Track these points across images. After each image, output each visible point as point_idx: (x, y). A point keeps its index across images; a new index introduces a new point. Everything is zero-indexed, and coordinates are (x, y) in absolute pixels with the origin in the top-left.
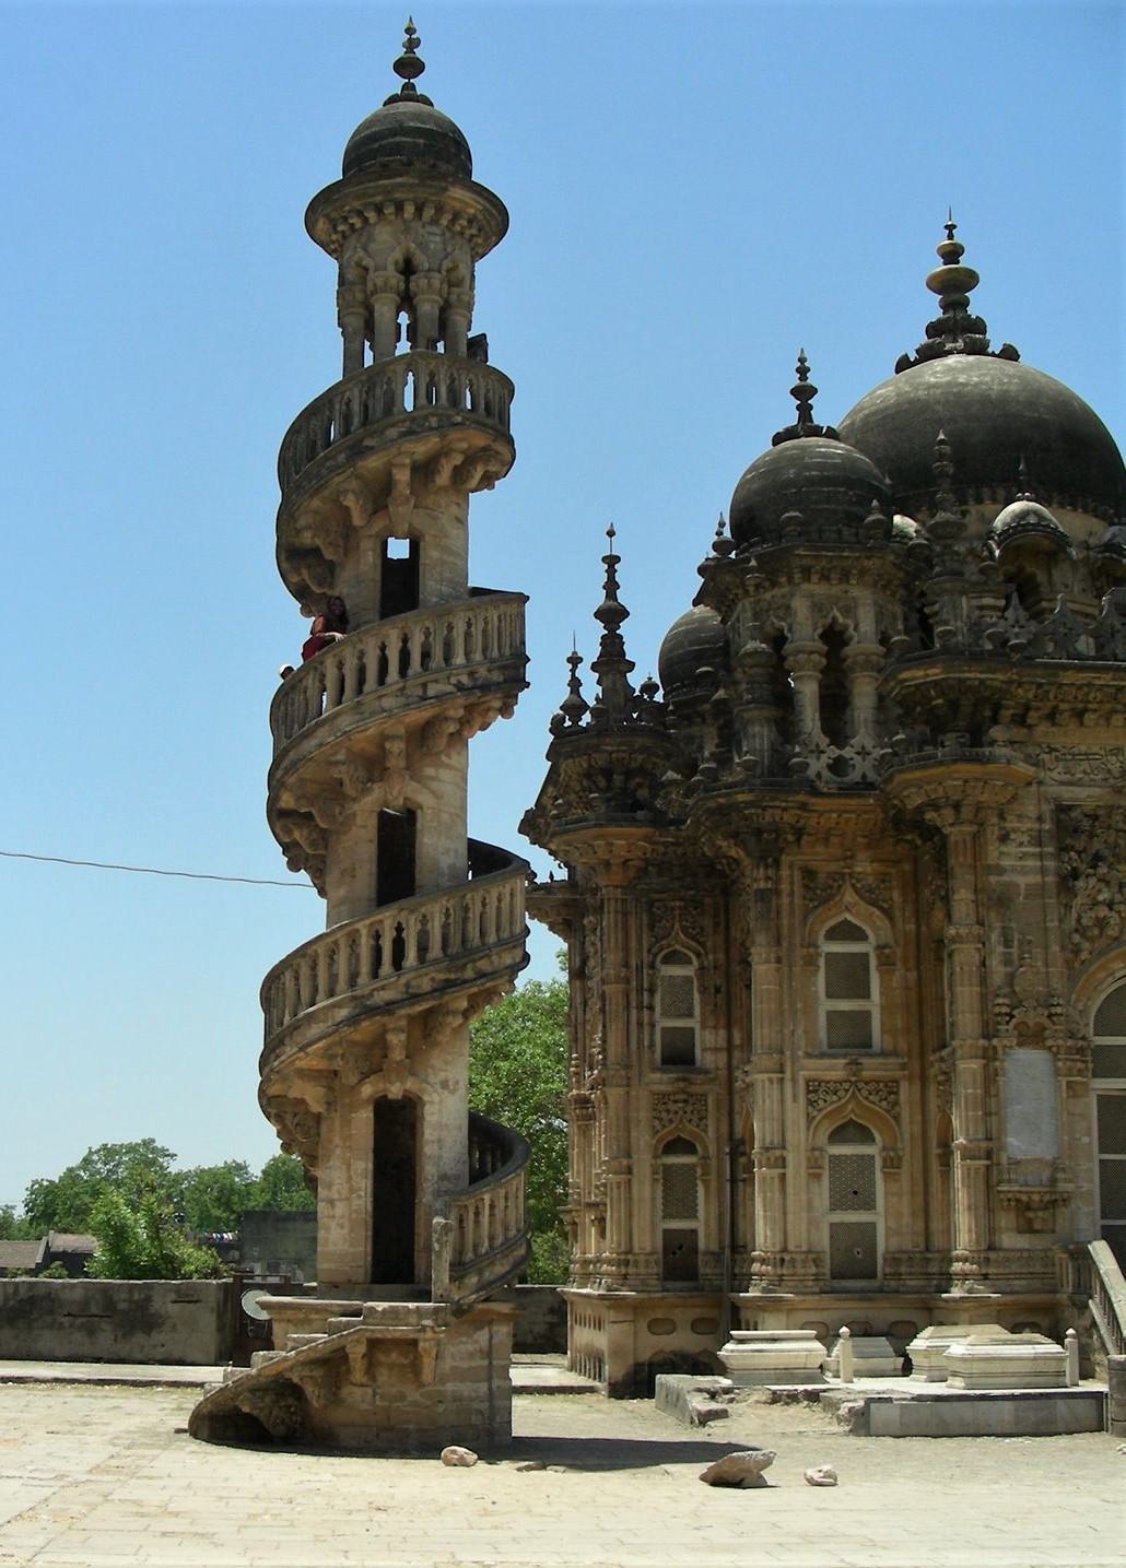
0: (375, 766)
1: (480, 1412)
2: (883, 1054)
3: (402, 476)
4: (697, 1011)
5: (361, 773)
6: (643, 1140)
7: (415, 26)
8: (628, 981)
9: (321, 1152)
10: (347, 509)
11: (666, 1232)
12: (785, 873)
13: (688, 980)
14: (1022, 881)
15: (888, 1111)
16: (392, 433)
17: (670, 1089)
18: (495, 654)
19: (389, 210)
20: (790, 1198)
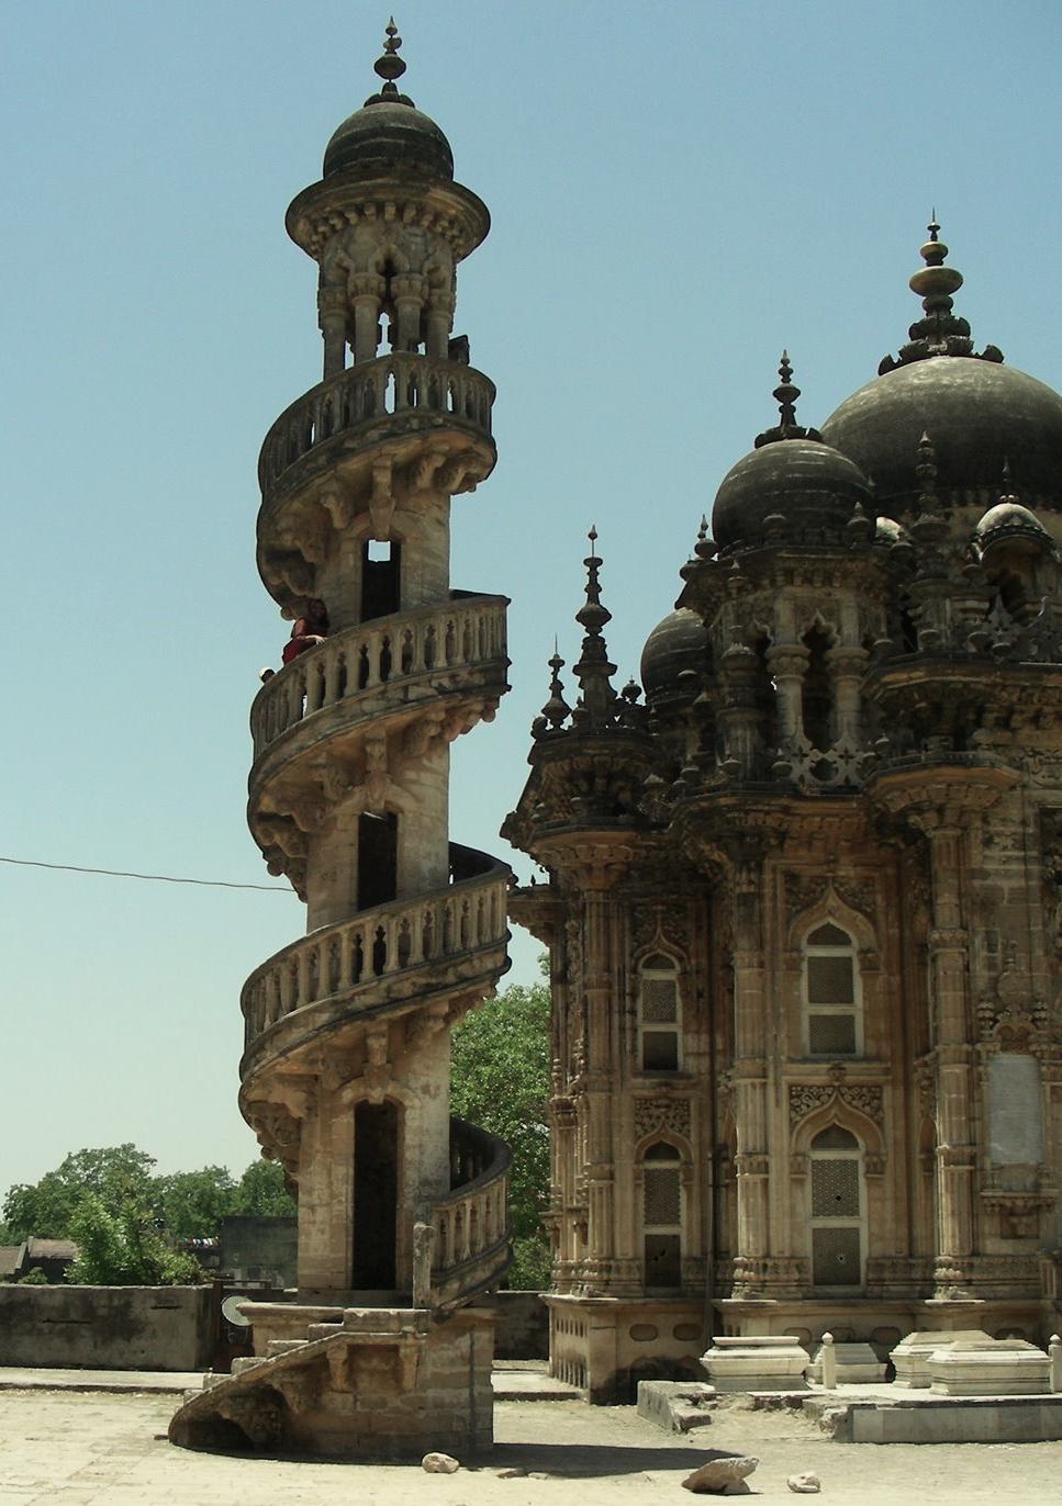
0: (355, 770)
1: (461, 1419)
2: (866, 1058)
3: (383, 478)
4: (679, 1015)
5: (342, 777)
6: (625, 1146)
7: (397, 26)
8: (610, 986)
9: (301, 1158)
10: (328, 510)
11: (648, 1238)
12: (767, 877)
13: (670, 984)
14: (1006, 885)
15: (872, 1117)
16: (374, 434)
17: (652, 1093)
18: (477, 656)
19: (370, 211)
20: (773, 1203)
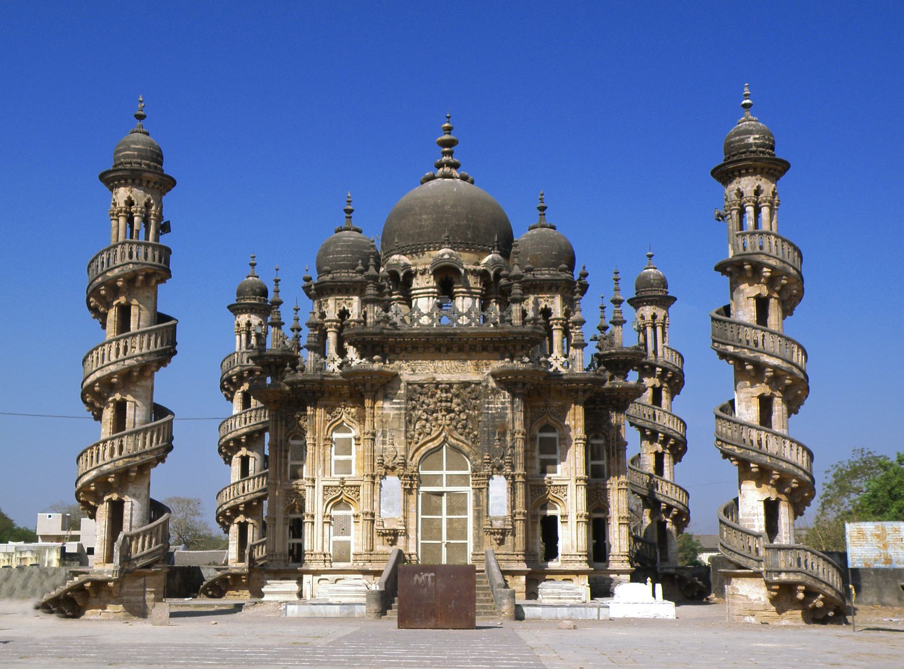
13: (301, 446)
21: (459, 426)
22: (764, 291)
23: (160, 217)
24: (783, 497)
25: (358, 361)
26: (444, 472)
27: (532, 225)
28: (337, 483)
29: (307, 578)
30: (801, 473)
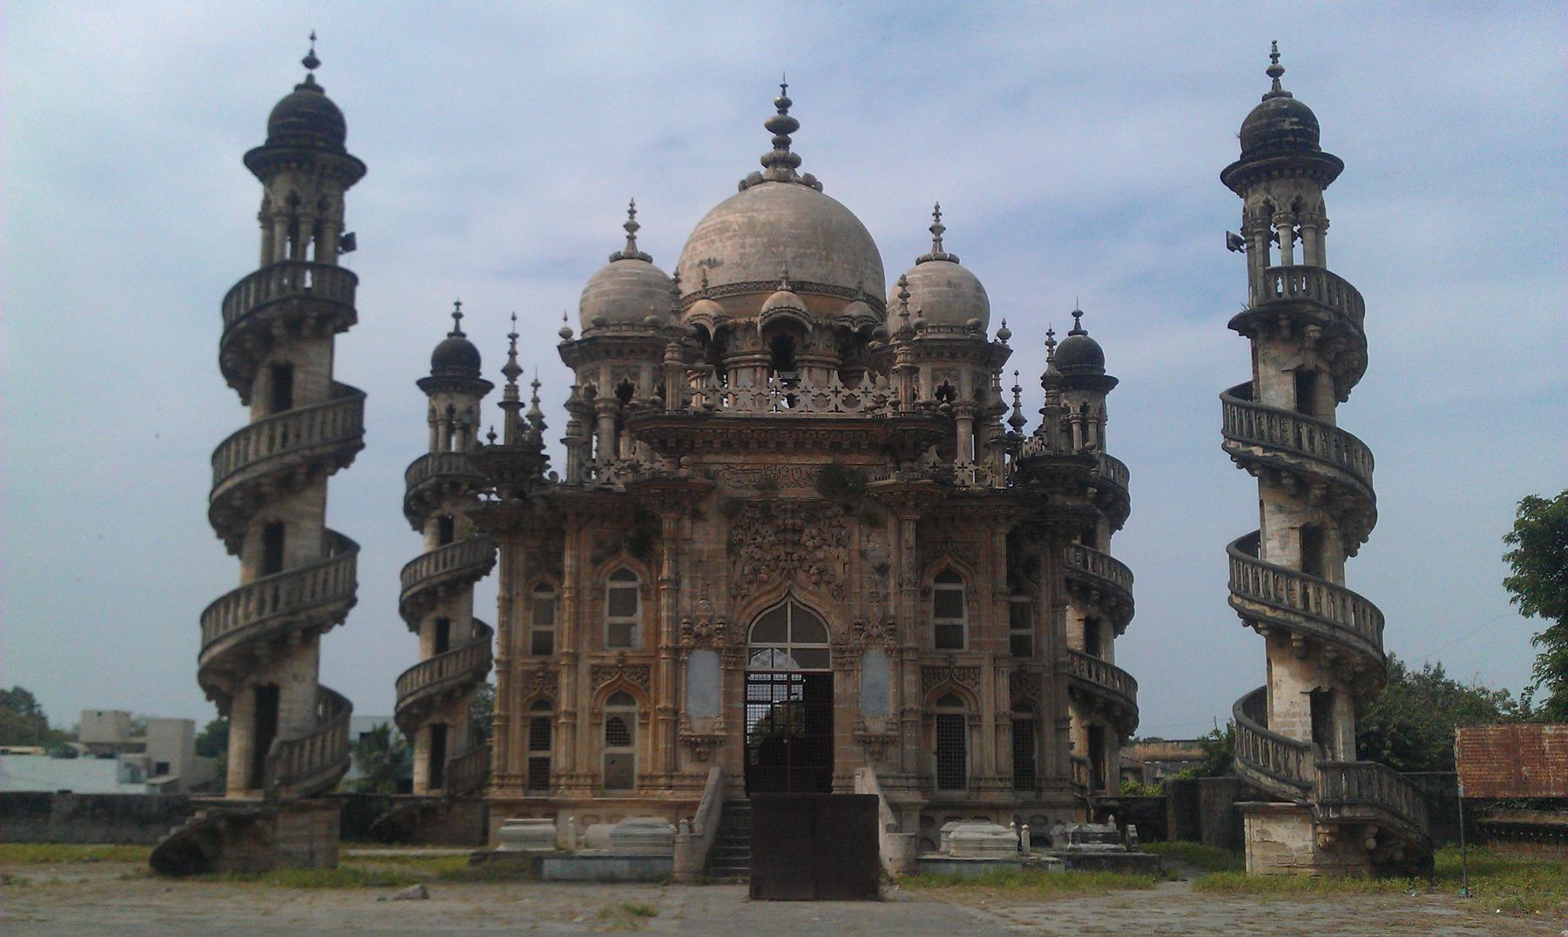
11: (531, 760)
13: (551, 601)
14: (706, 548)
21: (813, 570)
22: (1311, 361)
23: (341, 227)
24: (1340, 688)
25: (647, 465)
26: (789, 645)
27: (920, 255)
28: (612, 662)
29: (562, 814)
30: (1369, 649)
